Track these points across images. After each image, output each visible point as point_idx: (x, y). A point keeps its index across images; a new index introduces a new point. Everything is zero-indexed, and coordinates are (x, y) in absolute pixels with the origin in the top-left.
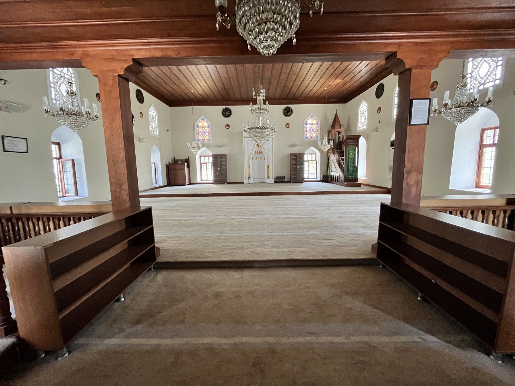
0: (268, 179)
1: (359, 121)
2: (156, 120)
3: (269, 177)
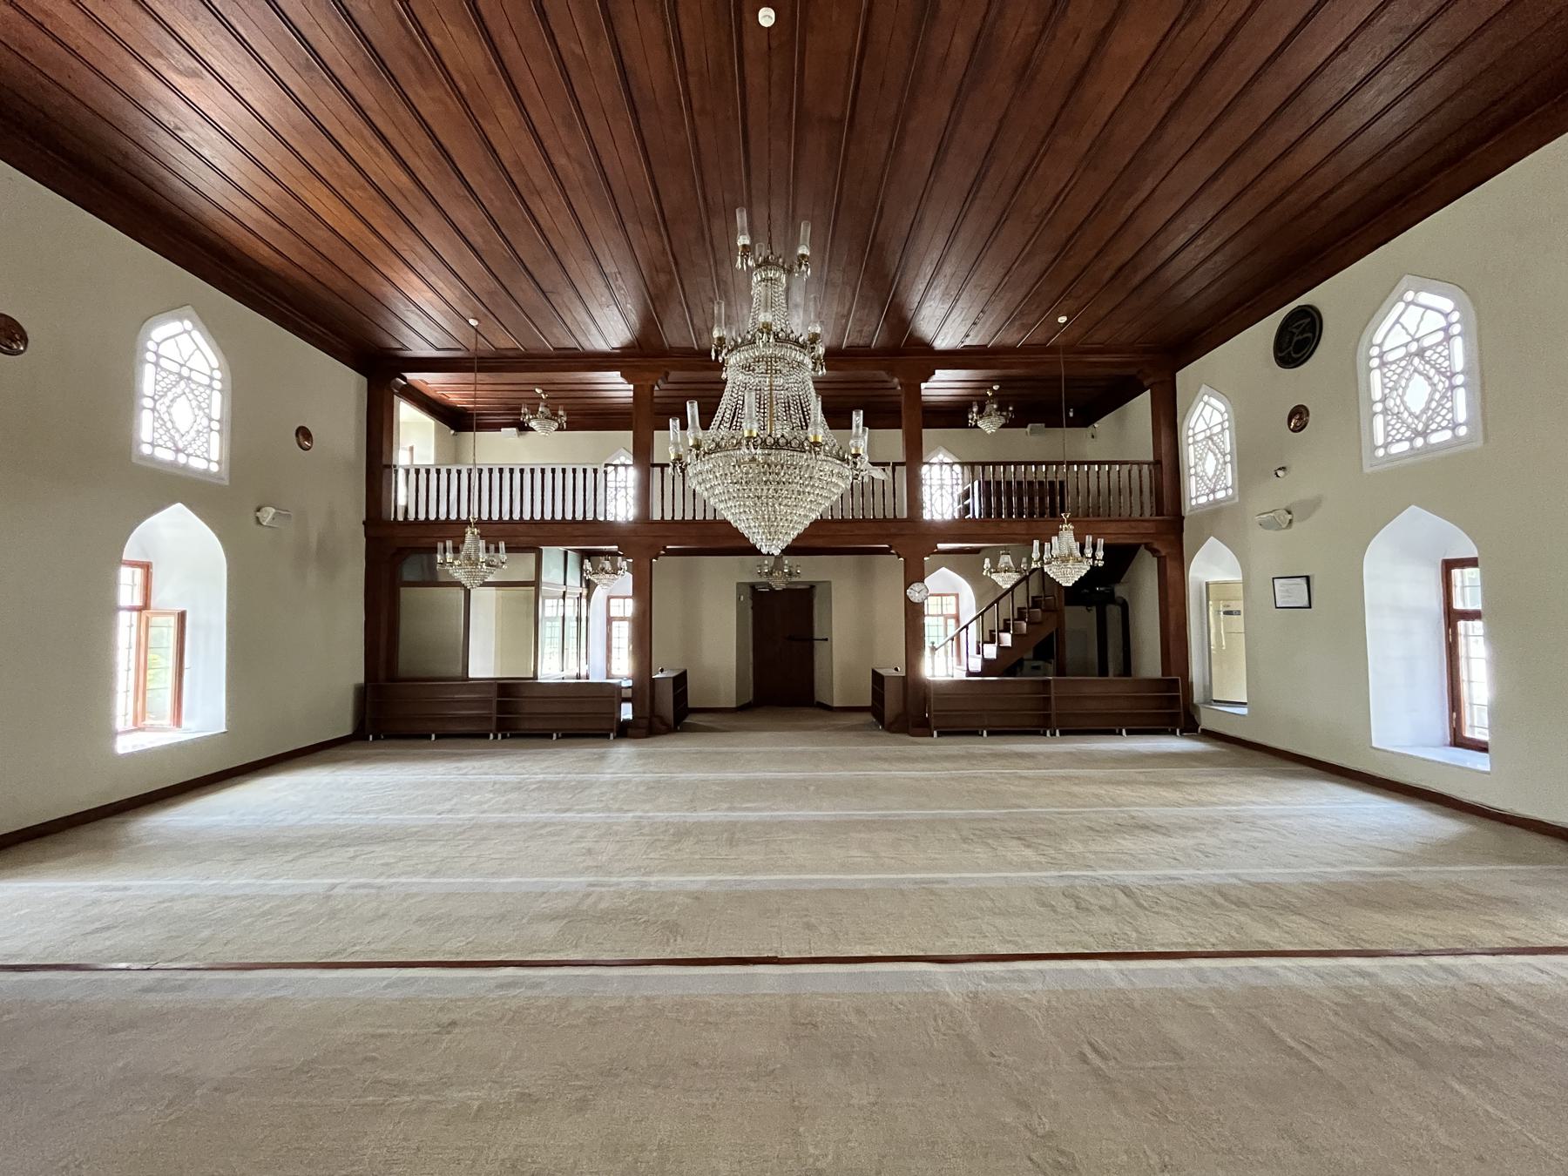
1: (1192, 471)
2: (210, 397)
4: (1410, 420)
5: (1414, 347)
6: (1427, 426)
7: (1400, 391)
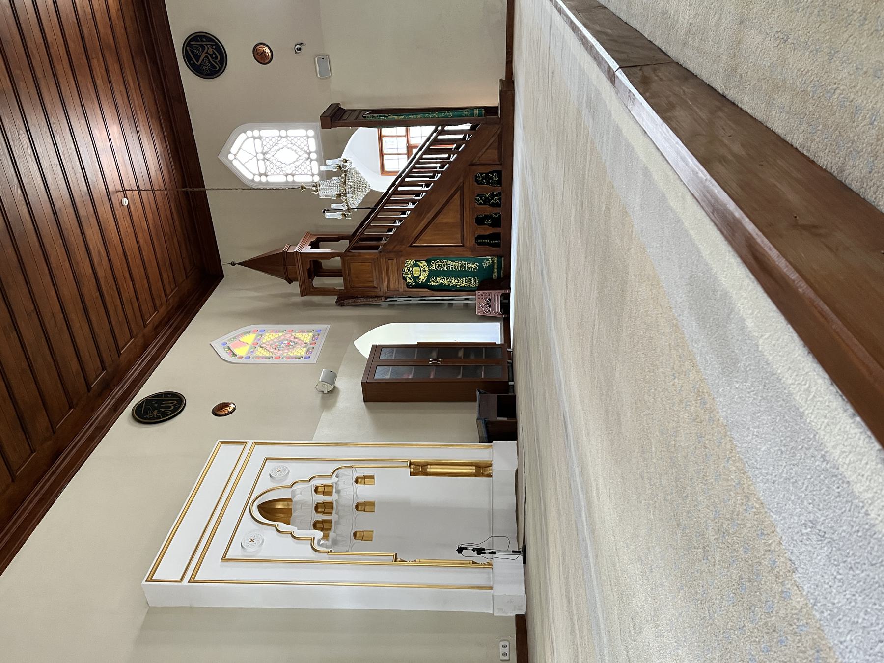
0: (496, 467)
3: (482, 470)
4: (301, 161)
5: (260, 156)
6: (306, 152)
7: (283, 165)
